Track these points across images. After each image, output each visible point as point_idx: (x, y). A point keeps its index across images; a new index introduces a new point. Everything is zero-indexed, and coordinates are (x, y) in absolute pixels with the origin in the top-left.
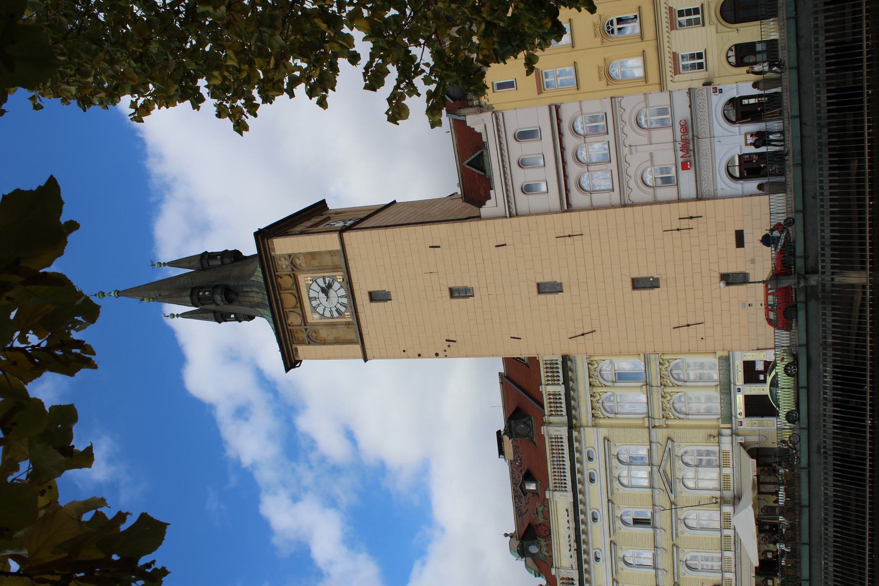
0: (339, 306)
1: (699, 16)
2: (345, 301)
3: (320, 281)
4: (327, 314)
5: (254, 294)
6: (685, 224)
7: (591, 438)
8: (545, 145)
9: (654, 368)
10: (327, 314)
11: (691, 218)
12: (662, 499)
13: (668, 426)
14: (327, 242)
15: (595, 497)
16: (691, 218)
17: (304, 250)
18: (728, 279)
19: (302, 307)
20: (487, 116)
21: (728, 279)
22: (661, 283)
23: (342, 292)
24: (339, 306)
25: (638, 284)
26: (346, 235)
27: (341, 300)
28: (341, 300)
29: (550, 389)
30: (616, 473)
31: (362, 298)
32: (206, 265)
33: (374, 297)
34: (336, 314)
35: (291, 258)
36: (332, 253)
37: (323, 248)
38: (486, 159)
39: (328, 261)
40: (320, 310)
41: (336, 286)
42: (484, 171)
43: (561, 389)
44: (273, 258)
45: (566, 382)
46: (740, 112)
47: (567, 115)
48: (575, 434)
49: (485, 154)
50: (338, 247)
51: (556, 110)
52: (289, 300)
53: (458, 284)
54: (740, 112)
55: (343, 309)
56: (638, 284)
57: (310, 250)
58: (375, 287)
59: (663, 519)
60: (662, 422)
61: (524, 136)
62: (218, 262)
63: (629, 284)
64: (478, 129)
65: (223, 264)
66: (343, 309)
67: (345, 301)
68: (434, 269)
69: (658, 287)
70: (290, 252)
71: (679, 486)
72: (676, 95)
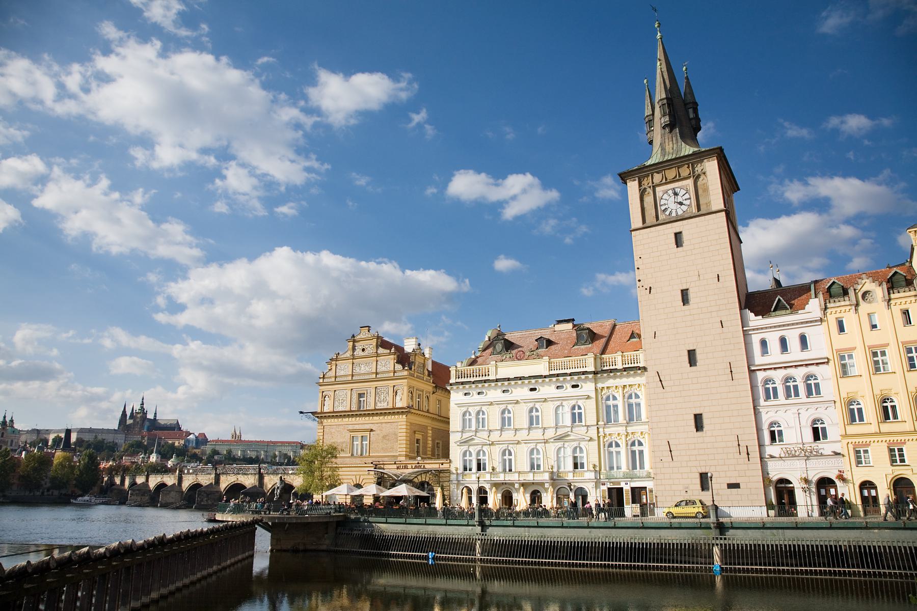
0: (669, 210)
1: (899, 463)
2: (674, 214)
3: (687, 196)
4: (663, 202)
5: (671, 145)
6: (743, 450)
10: (663, 202)
11: (748, 454)
12: (550, 434)
13: (599, 437)
14: (716, 199)
15: (548, 390)
16: (748, 454)
17: (709, 183)
19: (666, 183)
20: (818, 314)
22: (699, 433)
23: (680, 212)
24: (669, 210)
26: (724, 213)
27: (674, 212)
28: (674, 212)
30: (565, 403)
32: (688, 106)
33: (678, 237)
34: (663, 208)
36: (708, 204)
37: (712, 198)
38: (783, 312)
39: (702, 201)
40: (665, 196)
41: (684, 208)
42: (774, 311)
43: (619, 366)
44: (702, 161)
45: (625, 369)
48: (591, 376)
49: (788, 312)
50: (714, 209)
52: (671, 174)
53: (691, 295)
55: (667, 213)
57: (711, 188)
58: (685, 237)
60: (601, 434)
61: (803, 340)
62: (692, 116)
63: (698, 412)
64: (807, 306)
65: (691, 119)
66: (667, 213)
67: (674, 214)
68: (701, 277)
69: (697, 430)
70: (708, 173)
71: (560, 444)
72: (839, 444)
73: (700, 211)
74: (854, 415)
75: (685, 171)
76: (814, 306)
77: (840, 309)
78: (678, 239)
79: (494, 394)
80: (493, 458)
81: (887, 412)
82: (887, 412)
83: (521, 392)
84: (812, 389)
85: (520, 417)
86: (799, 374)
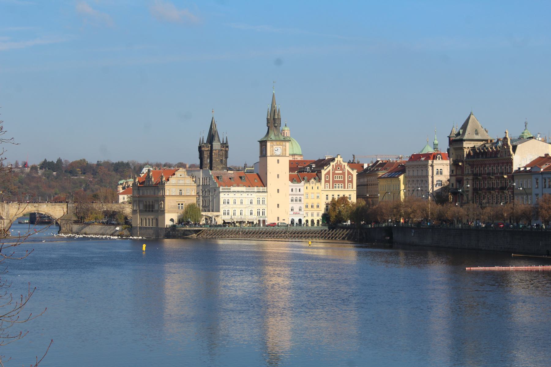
7: (254, 195)
8: (298, 193)
9: (265, 206)
15: (245, 195)
18: (278, 218)
21: (278, 218)
25: (278, 205)
29: (261, 189)
31: (278, 158)
33: (278, 160)
35: (286, 146)
46: (300, 220)
47: (302, 197)
51: (303, 195)
52: (278, 143)
53: (280, 176)
54: (300, 220)
56: (278, 205)
59: (241, 206)
73: (284, 155)
74: (307, 207)
75: (281, 143)
76: (303, 182)
77: (307, 185)
78: (278, 160)
79: (231, 195)
80: (231, 213)
81: (312, 207)
82: (312, 207)
83: (238, 195)
84: (300, 200)
85: (238, 202)
86: (298, 197)
